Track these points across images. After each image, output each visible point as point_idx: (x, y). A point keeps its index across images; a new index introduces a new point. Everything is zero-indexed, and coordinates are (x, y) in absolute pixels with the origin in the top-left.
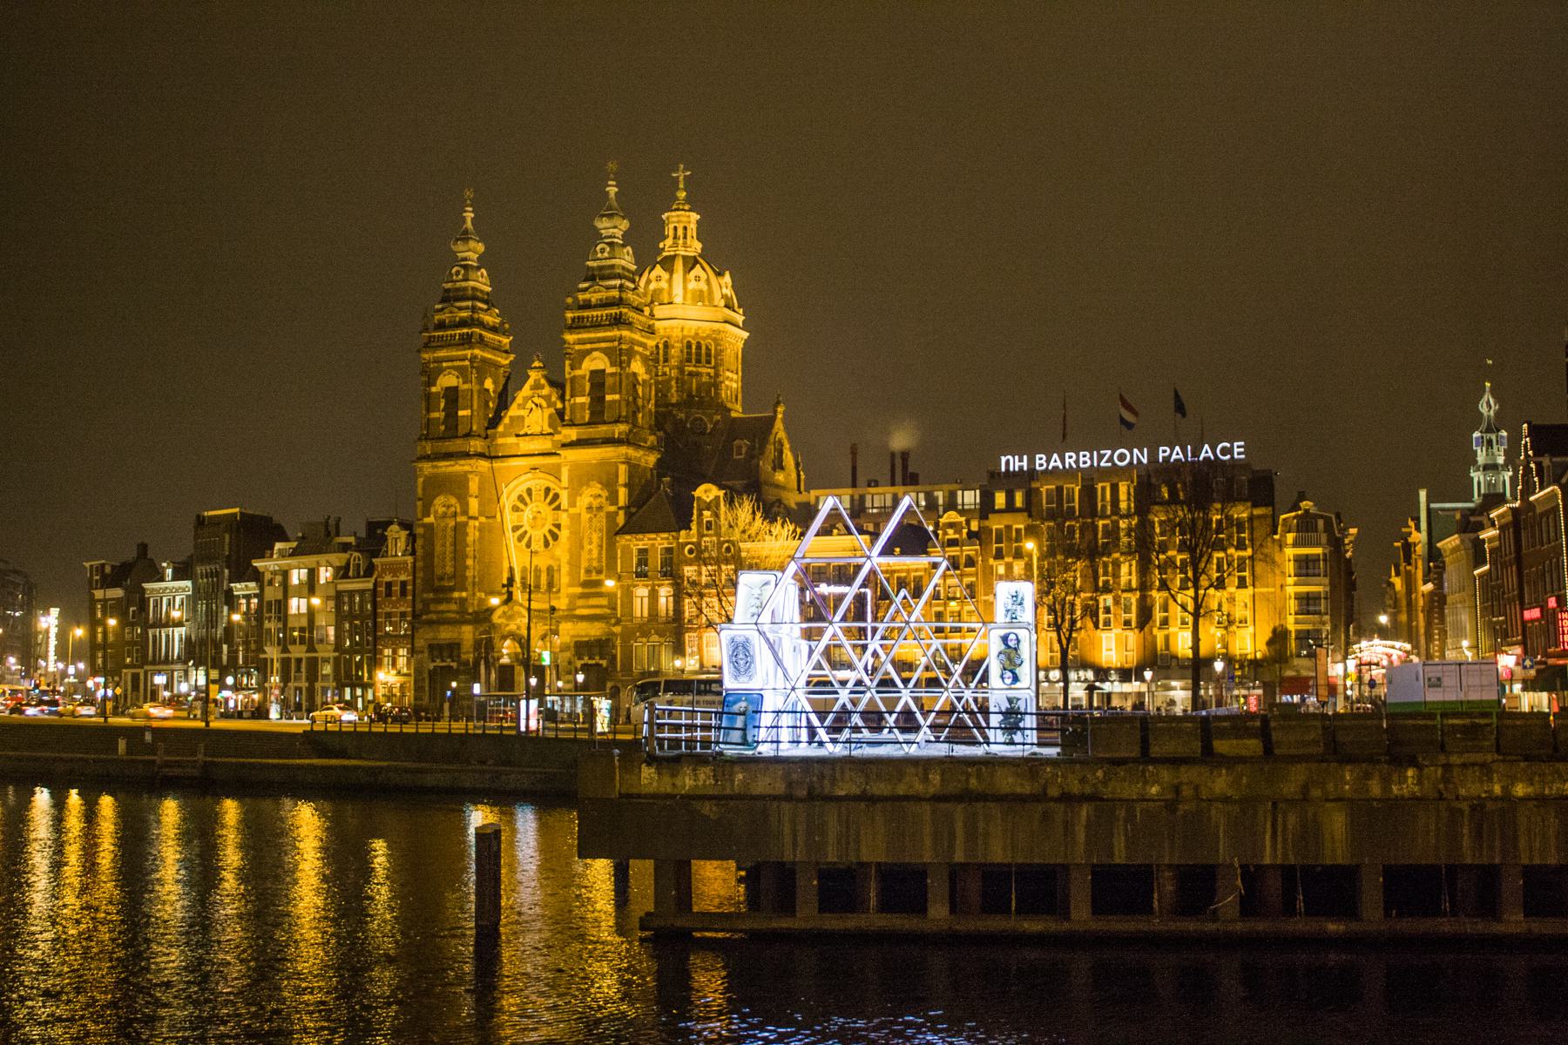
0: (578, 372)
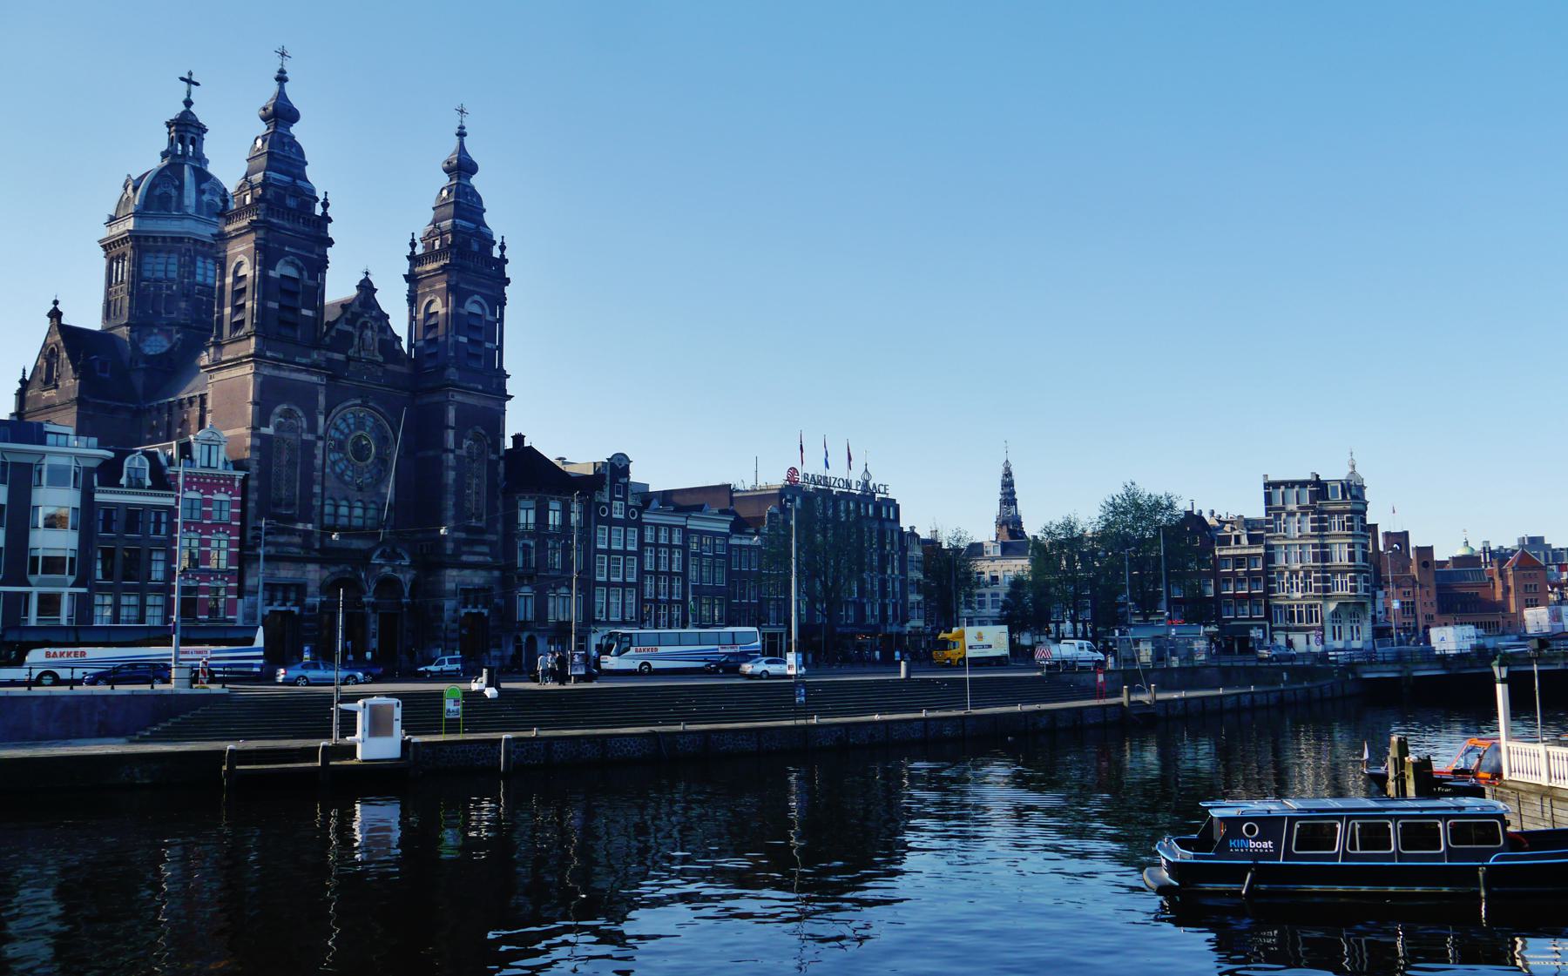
0: (461, 311)
